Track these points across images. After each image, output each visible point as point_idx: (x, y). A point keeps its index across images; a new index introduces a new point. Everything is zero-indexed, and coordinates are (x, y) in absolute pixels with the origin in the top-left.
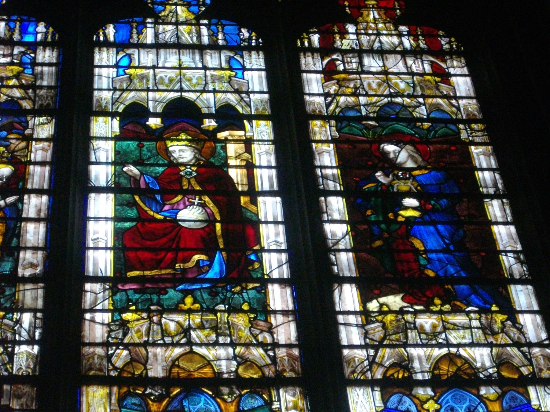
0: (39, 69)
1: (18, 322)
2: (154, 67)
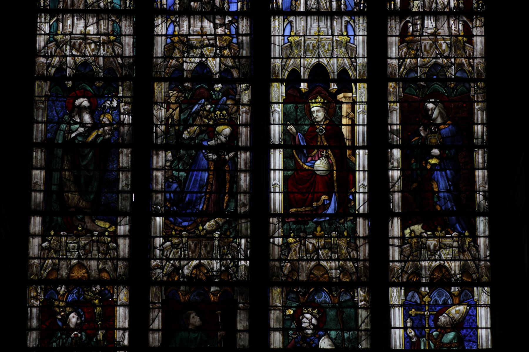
0: (240, 38)
1: (240, 244)
2: (305, 36)
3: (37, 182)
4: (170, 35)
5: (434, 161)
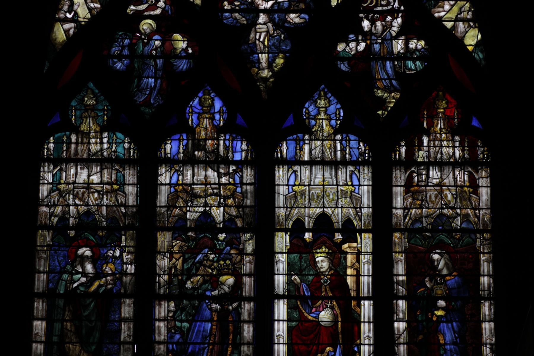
0: (245, 187)
3: (38, 333)
4: (173, 184)
5: (440, 313)
